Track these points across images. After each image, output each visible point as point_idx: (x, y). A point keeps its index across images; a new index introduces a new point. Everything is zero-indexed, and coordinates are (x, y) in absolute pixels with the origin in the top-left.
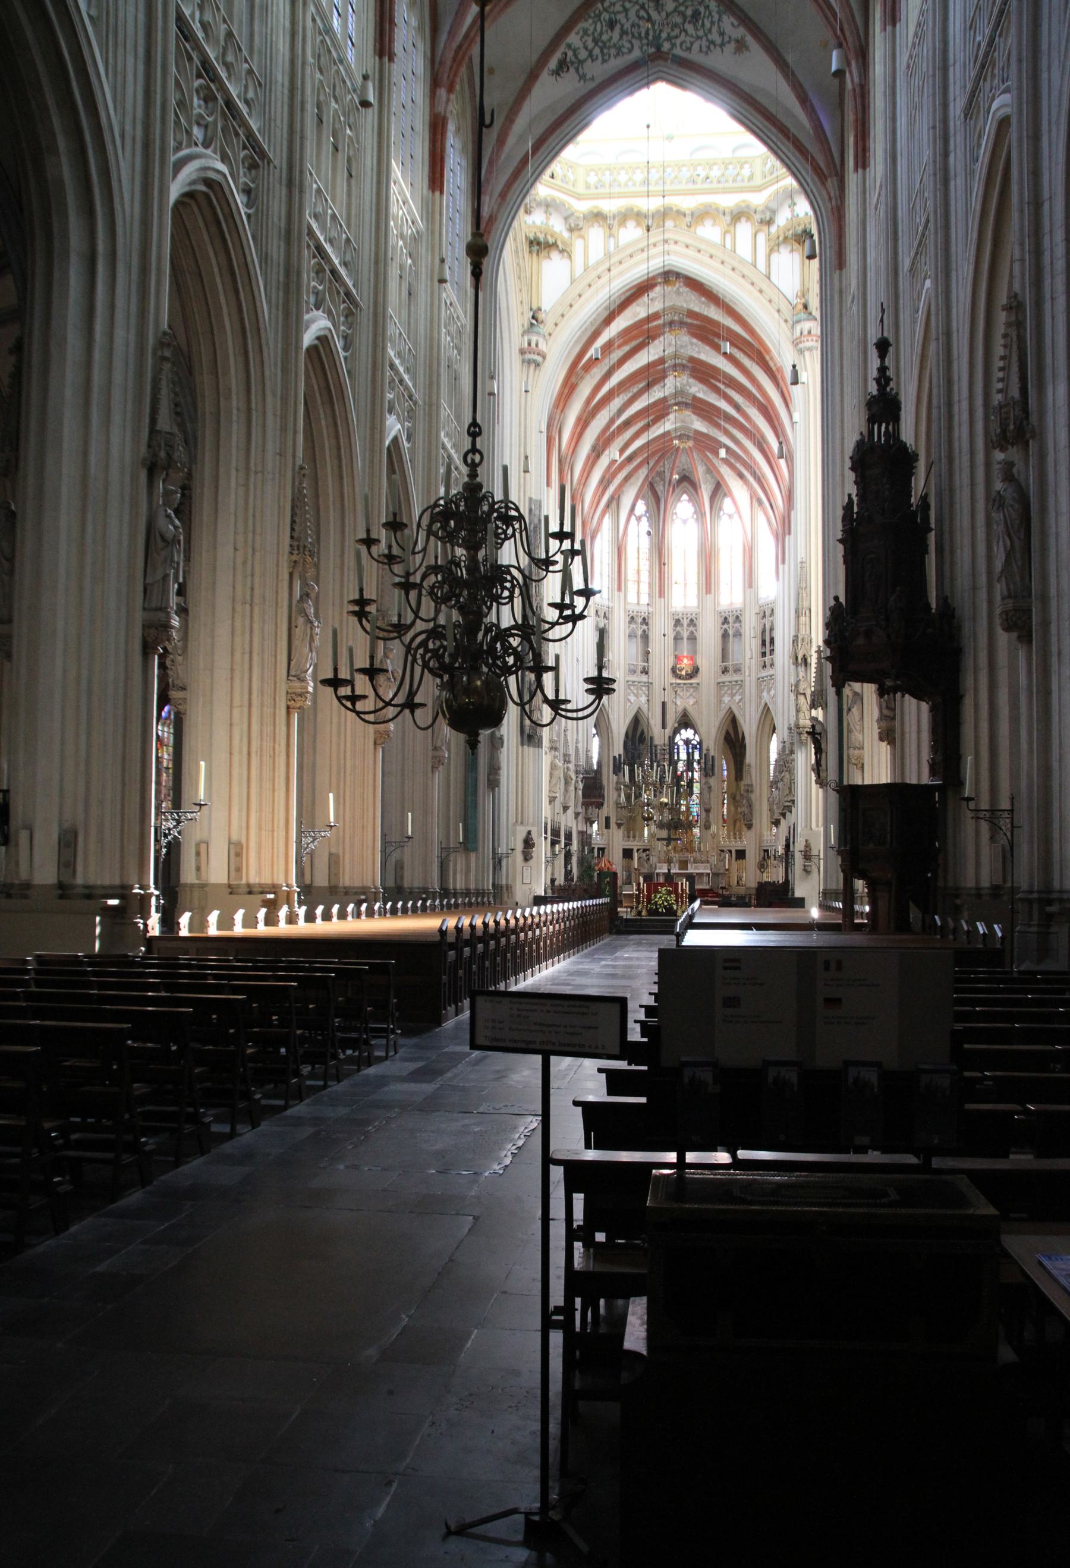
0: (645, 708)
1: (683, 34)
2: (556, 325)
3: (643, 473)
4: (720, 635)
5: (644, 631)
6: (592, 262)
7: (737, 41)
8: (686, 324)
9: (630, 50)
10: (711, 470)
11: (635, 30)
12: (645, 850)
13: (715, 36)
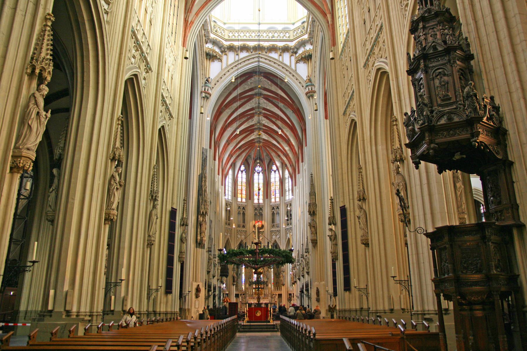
2: (215, 84)
3: (244, 155)
4: (271, 213)
5: (244, 212)
6: (229, 63)
8: (263, 94)
10: (269, 154)
12: (244, 294)
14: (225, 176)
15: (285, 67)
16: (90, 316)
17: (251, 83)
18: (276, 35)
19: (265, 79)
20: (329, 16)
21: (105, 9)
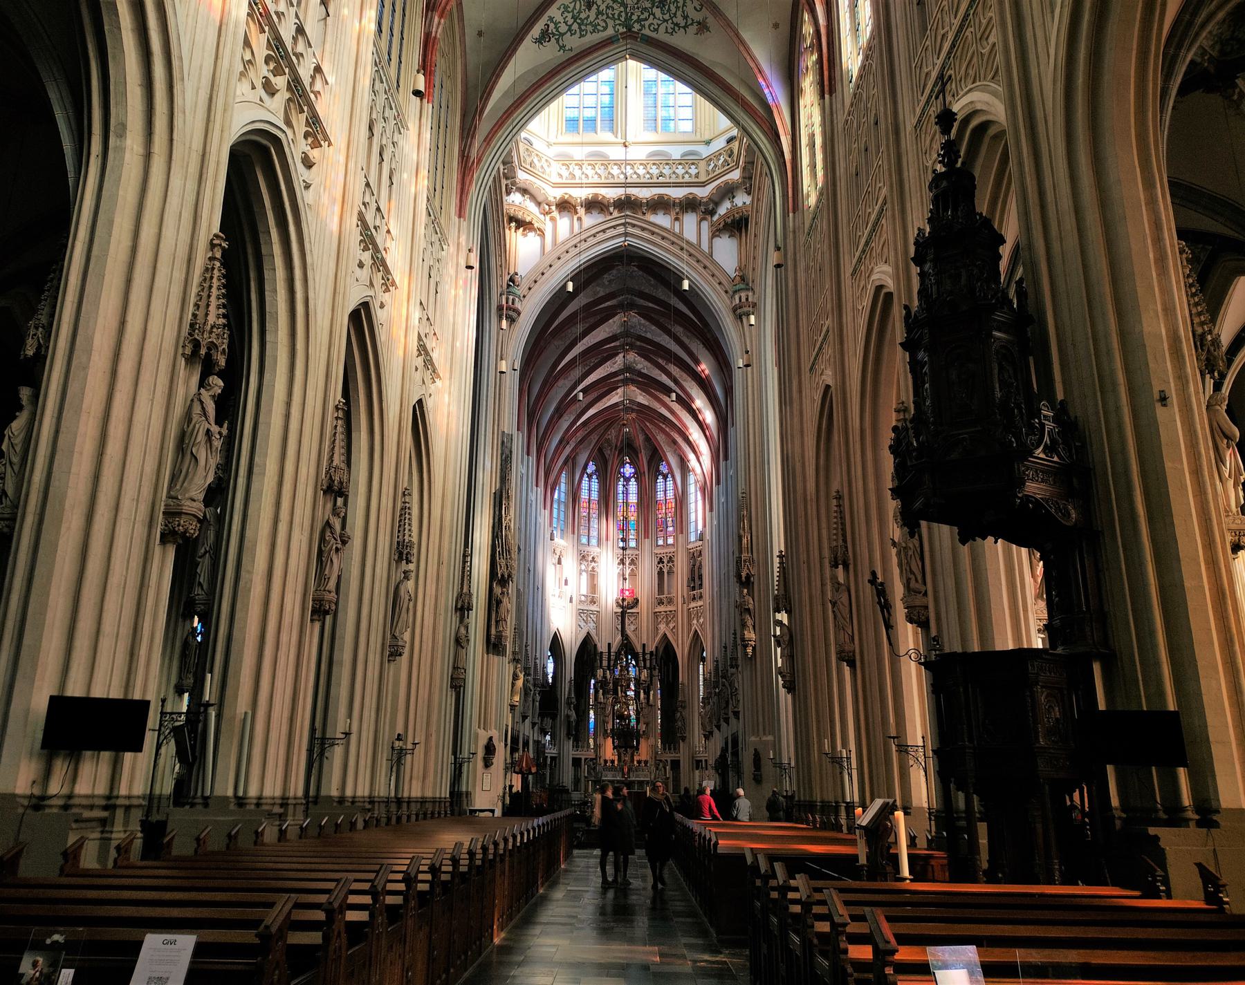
0: (593, 633)
1: (651, 16)
2: (530, 289)
3: (594, 438)
5: (593, 568)
7: (699, 23)
9: (605, 28)
11: (610, 12)
13: (679, 19)
14: (551, 487)
16: (282, 805)
17: (609, 281)
19: (641, 273)
21: (304, 181)
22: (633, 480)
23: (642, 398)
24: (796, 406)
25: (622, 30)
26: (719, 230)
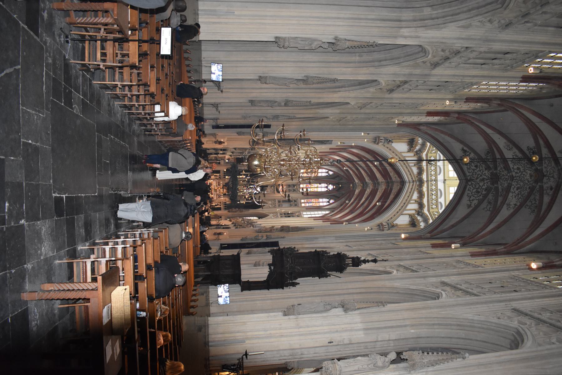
3: (342, 174)
7: (471, 205)
9: (469, 172)
11: (474, 174)
13: (472, 198)
15: (405, 205)
18: (434, 197)
20: (429, 235)
22: (327, 189)
23: (357, 191)
24: (335, 241)
25: (469, 178)
26: (412, 217)
